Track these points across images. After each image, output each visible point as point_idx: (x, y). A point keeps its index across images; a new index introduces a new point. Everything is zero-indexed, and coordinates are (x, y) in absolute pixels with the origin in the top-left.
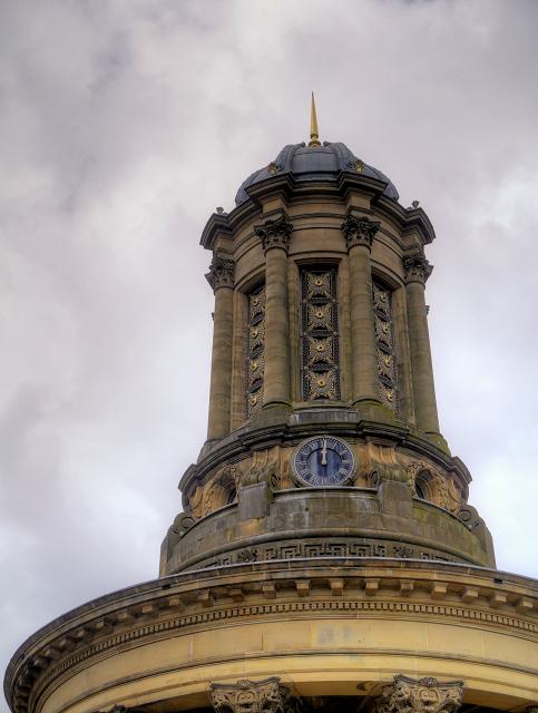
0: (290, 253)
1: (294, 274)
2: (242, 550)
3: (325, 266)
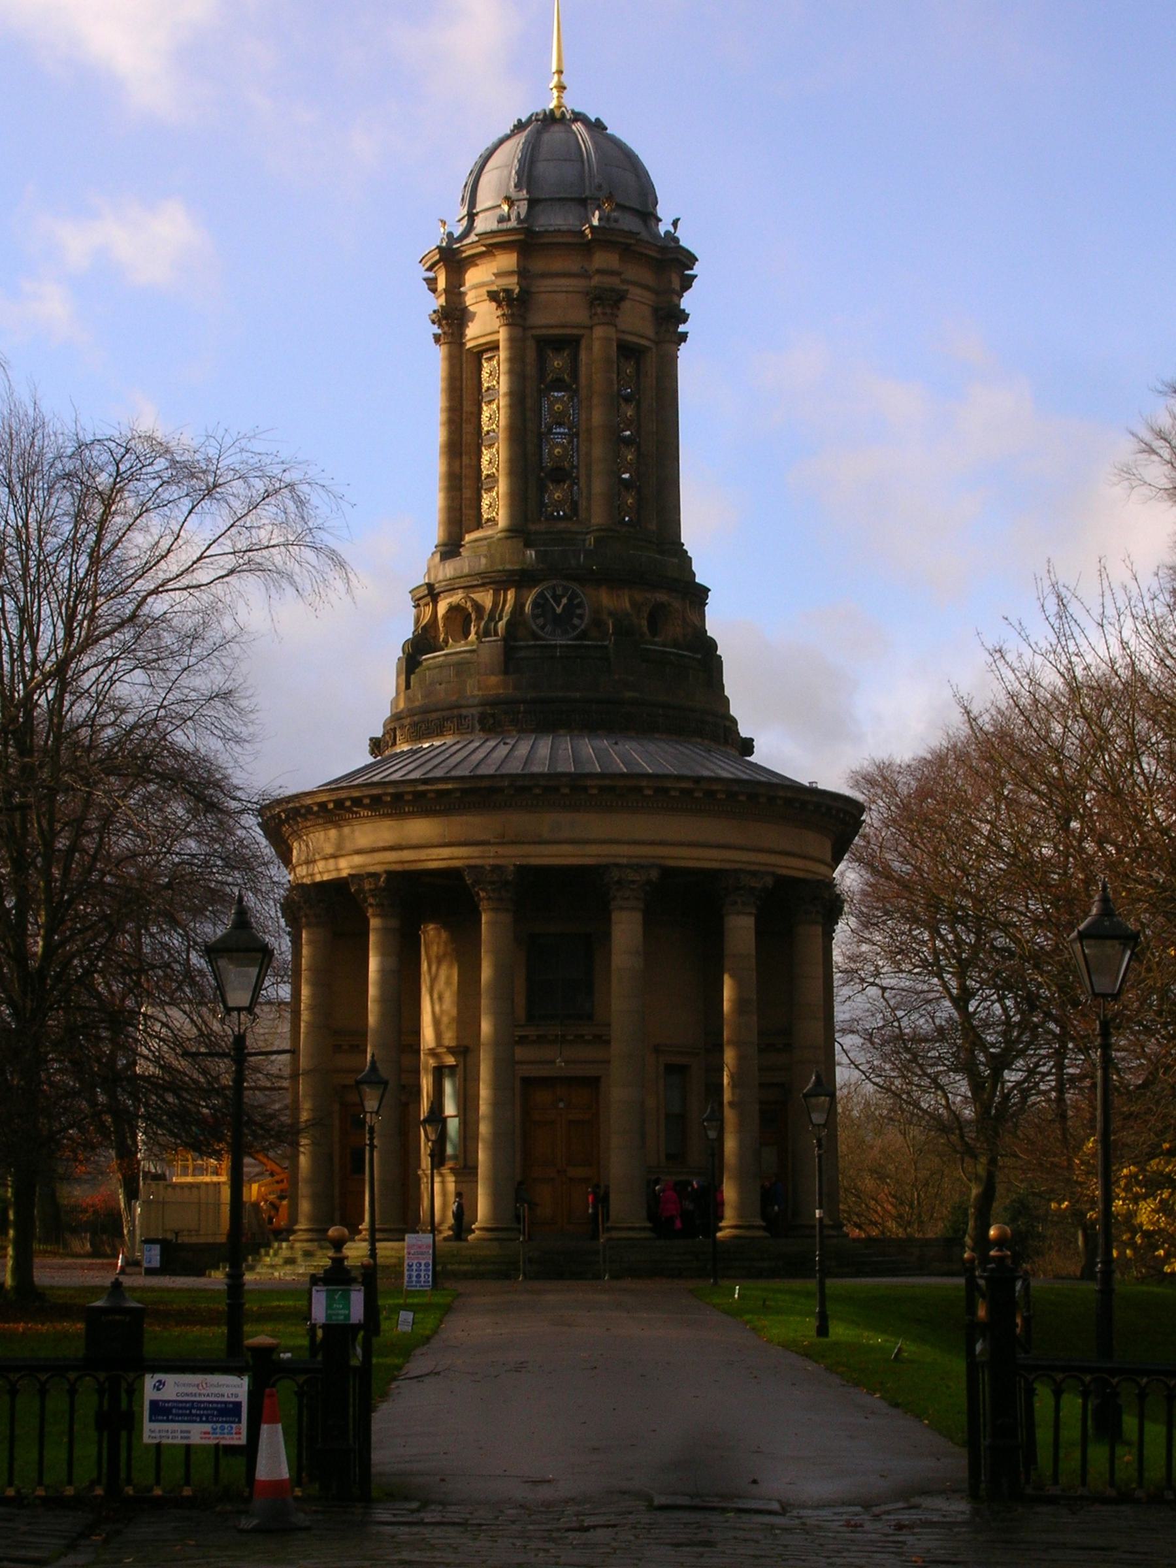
1: (531, 355)
3: (568, 343)
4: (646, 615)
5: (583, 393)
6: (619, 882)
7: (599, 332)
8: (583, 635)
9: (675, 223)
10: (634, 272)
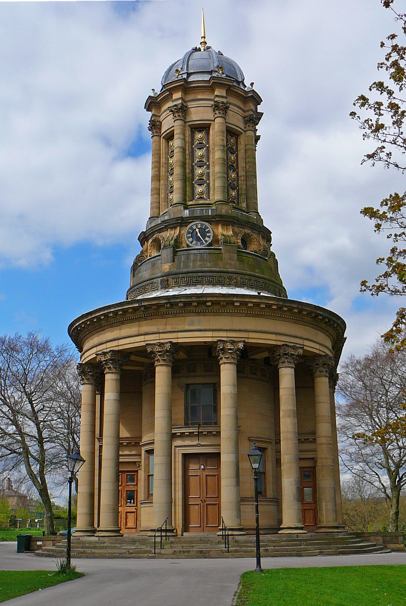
0: (186, 121)
1: (188, 133)
2: (162, 278)
3: (205, 128)
4: (240, 238)
5: (211, 149)
6: (222, 350)
7: (217, 120)
8: (210, 244)
9: (252, 84)
10: (232, 100)
